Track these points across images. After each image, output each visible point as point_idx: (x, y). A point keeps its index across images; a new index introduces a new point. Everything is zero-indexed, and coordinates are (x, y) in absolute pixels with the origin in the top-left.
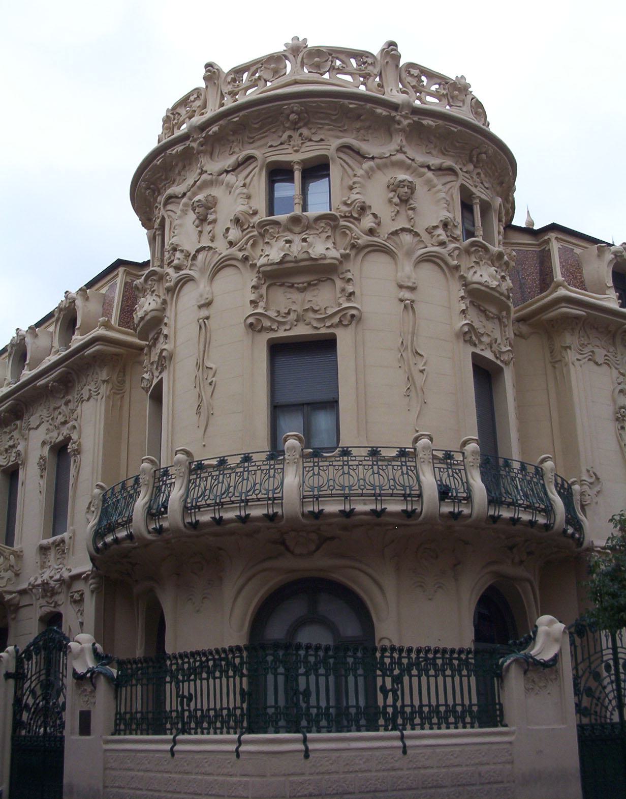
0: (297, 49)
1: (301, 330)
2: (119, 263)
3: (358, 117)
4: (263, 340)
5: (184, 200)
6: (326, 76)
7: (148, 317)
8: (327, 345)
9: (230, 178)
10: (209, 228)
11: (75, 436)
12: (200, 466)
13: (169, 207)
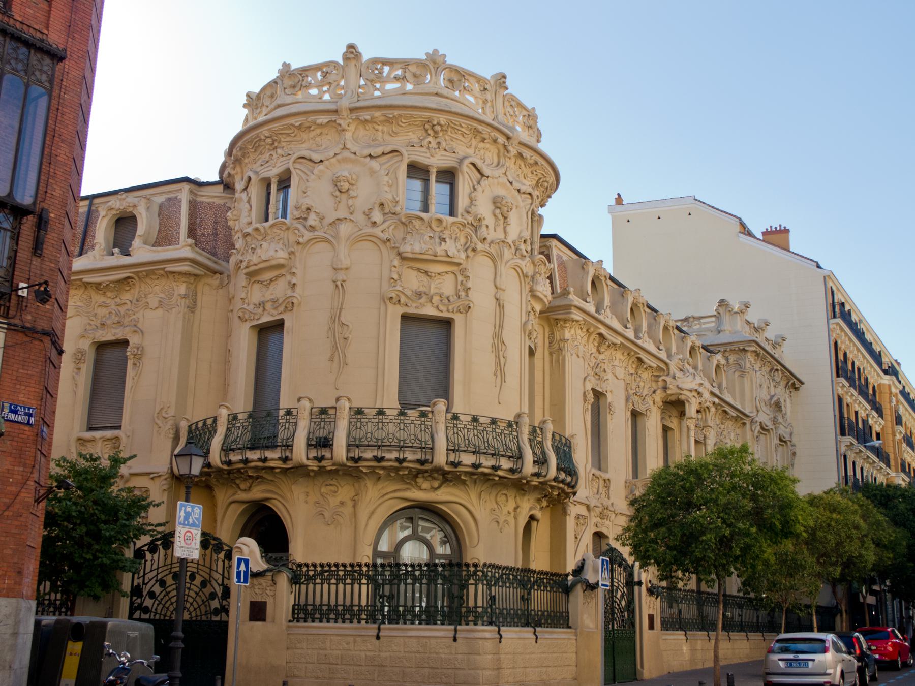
0: (434, 62)
2: (186, 180)
3: (483, 140)
5: (321, 167)
6: (457, 93)
7: (274, 262)
8: (447, 324)
9: (374, 164)
10: (350, 202)
11: (134, 340)
12: (359, 412)
13: (297, 166)
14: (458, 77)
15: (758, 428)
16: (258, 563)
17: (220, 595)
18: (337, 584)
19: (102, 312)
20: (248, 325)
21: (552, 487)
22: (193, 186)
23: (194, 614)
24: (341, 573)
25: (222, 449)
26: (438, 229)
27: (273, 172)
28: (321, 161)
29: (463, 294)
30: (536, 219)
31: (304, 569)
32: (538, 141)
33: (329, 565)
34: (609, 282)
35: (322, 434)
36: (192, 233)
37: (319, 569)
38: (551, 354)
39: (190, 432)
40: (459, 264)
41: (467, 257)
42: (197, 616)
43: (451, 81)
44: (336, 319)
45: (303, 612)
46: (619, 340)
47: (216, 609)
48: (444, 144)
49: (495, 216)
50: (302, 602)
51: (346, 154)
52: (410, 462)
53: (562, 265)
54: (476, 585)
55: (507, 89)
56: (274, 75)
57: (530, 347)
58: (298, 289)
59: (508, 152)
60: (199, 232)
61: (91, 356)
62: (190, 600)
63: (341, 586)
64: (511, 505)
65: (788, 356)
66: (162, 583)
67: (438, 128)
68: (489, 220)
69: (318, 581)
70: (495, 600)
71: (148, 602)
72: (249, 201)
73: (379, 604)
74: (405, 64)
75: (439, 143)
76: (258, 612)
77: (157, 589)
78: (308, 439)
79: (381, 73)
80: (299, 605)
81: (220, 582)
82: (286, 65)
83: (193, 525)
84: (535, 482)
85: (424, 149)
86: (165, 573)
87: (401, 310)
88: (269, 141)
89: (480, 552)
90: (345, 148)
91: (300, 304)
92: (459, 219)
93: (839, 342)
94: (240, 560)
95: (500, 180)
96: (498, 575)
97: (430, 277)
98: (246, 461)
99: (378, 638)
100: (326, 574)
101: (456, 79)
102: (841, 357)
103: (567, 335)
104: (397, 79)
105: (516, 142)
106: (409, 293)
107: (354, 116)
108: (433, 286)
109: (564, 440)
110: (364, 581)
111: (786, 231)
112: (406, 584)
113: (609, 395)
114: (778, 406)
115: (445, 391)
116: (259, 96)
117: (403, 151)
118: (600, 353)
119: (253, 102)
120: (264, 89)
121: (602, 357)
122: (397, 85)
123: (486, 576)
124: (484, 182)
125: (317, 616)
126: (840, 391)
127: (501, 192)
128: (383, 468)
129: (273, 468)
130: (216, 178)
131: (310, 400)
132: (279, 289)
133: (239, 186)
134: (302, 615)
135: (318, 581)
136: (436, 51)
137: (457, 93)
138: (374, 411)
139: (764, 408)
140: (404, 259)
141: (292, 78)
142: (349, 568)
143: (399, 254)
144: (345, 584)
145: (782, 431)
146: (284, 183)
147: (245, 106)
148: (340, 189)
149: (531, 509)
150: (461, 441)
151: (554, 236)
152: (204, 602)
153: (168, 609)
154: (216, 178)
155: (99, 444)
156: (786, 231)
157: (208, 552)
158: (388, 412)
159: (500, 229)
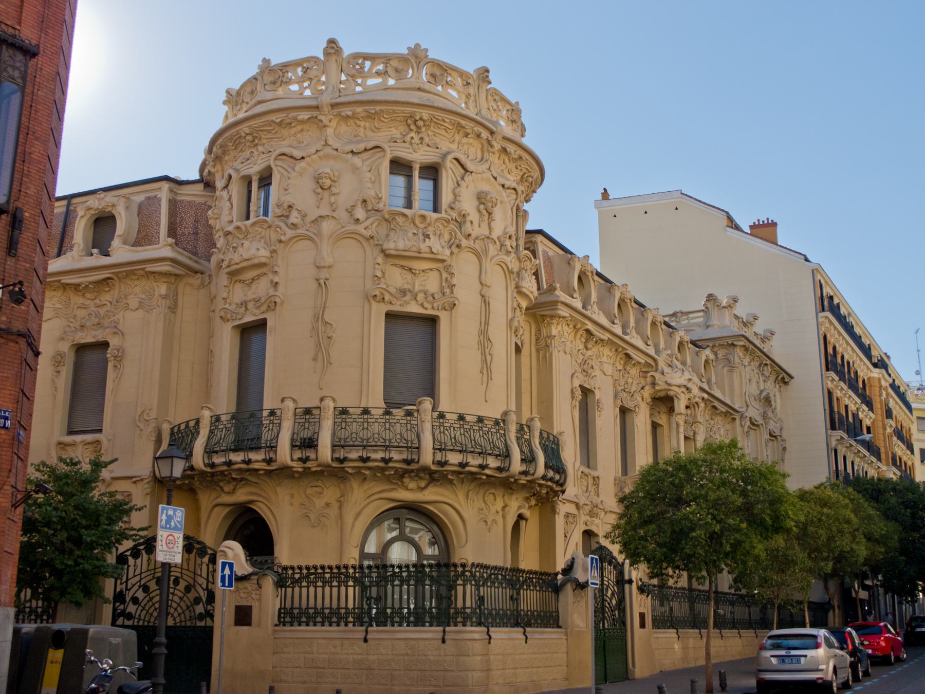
0: (416, 56)
1: (414, 308)
2: (166, 178)
3: (467, 135)
4: (379, 311)
5: (303, 164)
6: (439, 88)
7: (256, 261)
8: (432, 322)
9: (357, 160)
10: (333, 199)
11: (114, 342)
12: (344, 411)
13: (279, 163)
14: (440, 71)
15: (748, 423)
16: (243, 566)
17: (204, 600)
18: (323, 587)
19: (82, 313)
20: (230, 325)
21: (541, 485)
22: (172, 185)
23: (178, 620)
24: (327, 576)
25: (205, 452)
26: (422, 226)
27: (254, 169)
28: (303, 158)
29: (448, 291)
30: (520, 215)
31: (290, 572)
32: (523, 136)
33: (315, 568)
34: (596, 278)
35: (306, 434)
36: (172, 232)
37: (305, 571)
38: (538, 351)
39: (172, 434)
40: (443, 261)
41: (452, 253)
42: (181, 622)
43: (433, 76)
44: (319, 317)
45: (289, 616)
46: (606, 336)
47: (200, 614)
48: (426, 140)
49: (479, 211)
50: (288, 605)
51: (328, 150)
52: (396, 461)
53: (548, 260)
54: (464, 585)
55: (490, 83)
56: (254, 71)
57: (516, 344)
58: (281, 288)
59: (492, 146)
60: (179, 232)
61: (70, 359)
62: (174, 605)
63: (327, 589)
64: (499, 504)
65: (777, 350)
66: (146, 589)
67: (420, 123)
68: (473, 216)
69: (304, 584)
70: (483, 601)
71: (131, 608)
72: (230, 199)
73: (366, 607)
74: (386, 58)
75: (422, 139)
76: (243, 616)
77: (140, 595)
78: (292, 440)
79: (362, 68)
80: (285, 608)
81: (204, 586)
82: (266, 61)
83: (176, 528)
84: (523, 480)
85: (406, 145)
86: (148, 578)
87: (385, 308)
88: (249, 138)
89: (468, 553)
90: (326, 144)
91: (282, 304)
92: (443, 215)
93: (828, 336)
94: (224, 564)
95: (484, 175)
96: (487, 575)
97: (415, 274)
98: (230, 463)
99: (366, 640)
100: (312, 577)
101: (438, 74)
102: (830, 350)
103: (554, 331)
104: (378, 74)
105: (500, 137)
106: (393, 291)
107: (335, 111)
108: (417, 283)
109: (551, 438)
110: (351, 583)
111: (774, 224)
112: (393, 586)
113: (597, 392)
114: (768, 401)
115: (431, 390)
116: (238, 93)
117: (386, 146)
118: (587, 349)
119: (233, 99)
120: (243, 86)
121: (589, 353)
122: (378, 80)
123: (475, 576)
124: (468, 178)
125: (304, 619)
126: (830, 385)
127: (485, 187)
128: (369, 468)
129: (258, 470)
130: (197, 177)
131: (294, 400)
132: (262, 288)
133: (219, 184)
134: (288, 619)
135: (304, 584)
136: (417, 45)
137: (439, 88)
138: (359, 411)
139: (754, 403)
140: (387, 256)
141: (273, 74)
142: (335, 571)
143: (383, 251)
144: (331, 587)
145: (772, 425)
146: (265, 180)
147: (225, 103)
148: (322, 186)
149: (519, 508)
150: (448, 440)
151: (540, 232)
152: (188, 607)
153: (151, 615)
154: (197, 177)
155: (80, 447)
156: (774, 224)
157: (192, 556)
158: (373, 411)
159: (485, 225)
